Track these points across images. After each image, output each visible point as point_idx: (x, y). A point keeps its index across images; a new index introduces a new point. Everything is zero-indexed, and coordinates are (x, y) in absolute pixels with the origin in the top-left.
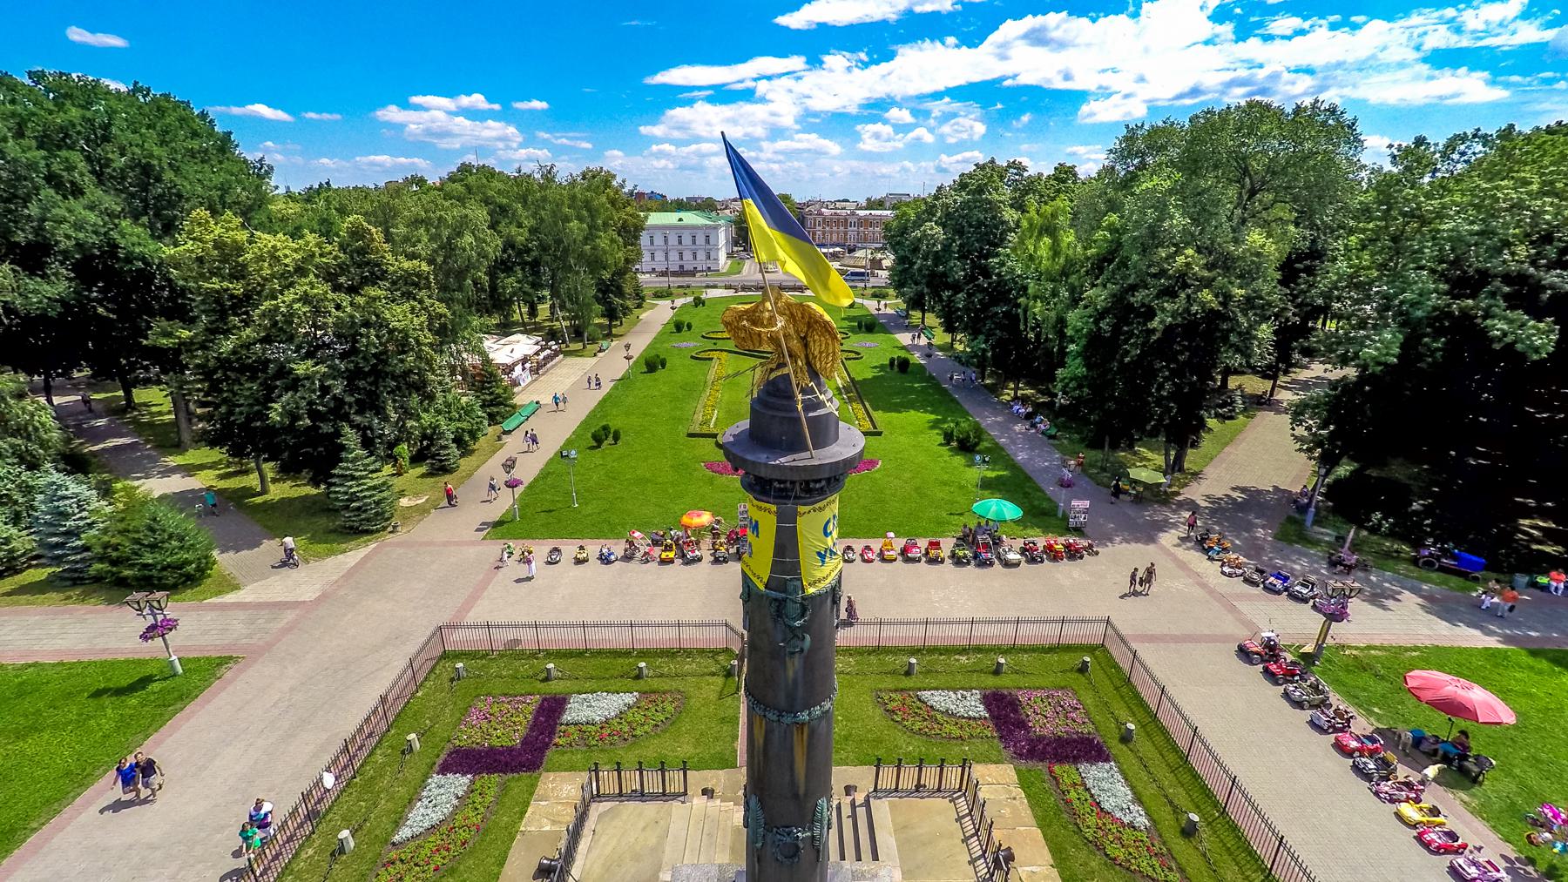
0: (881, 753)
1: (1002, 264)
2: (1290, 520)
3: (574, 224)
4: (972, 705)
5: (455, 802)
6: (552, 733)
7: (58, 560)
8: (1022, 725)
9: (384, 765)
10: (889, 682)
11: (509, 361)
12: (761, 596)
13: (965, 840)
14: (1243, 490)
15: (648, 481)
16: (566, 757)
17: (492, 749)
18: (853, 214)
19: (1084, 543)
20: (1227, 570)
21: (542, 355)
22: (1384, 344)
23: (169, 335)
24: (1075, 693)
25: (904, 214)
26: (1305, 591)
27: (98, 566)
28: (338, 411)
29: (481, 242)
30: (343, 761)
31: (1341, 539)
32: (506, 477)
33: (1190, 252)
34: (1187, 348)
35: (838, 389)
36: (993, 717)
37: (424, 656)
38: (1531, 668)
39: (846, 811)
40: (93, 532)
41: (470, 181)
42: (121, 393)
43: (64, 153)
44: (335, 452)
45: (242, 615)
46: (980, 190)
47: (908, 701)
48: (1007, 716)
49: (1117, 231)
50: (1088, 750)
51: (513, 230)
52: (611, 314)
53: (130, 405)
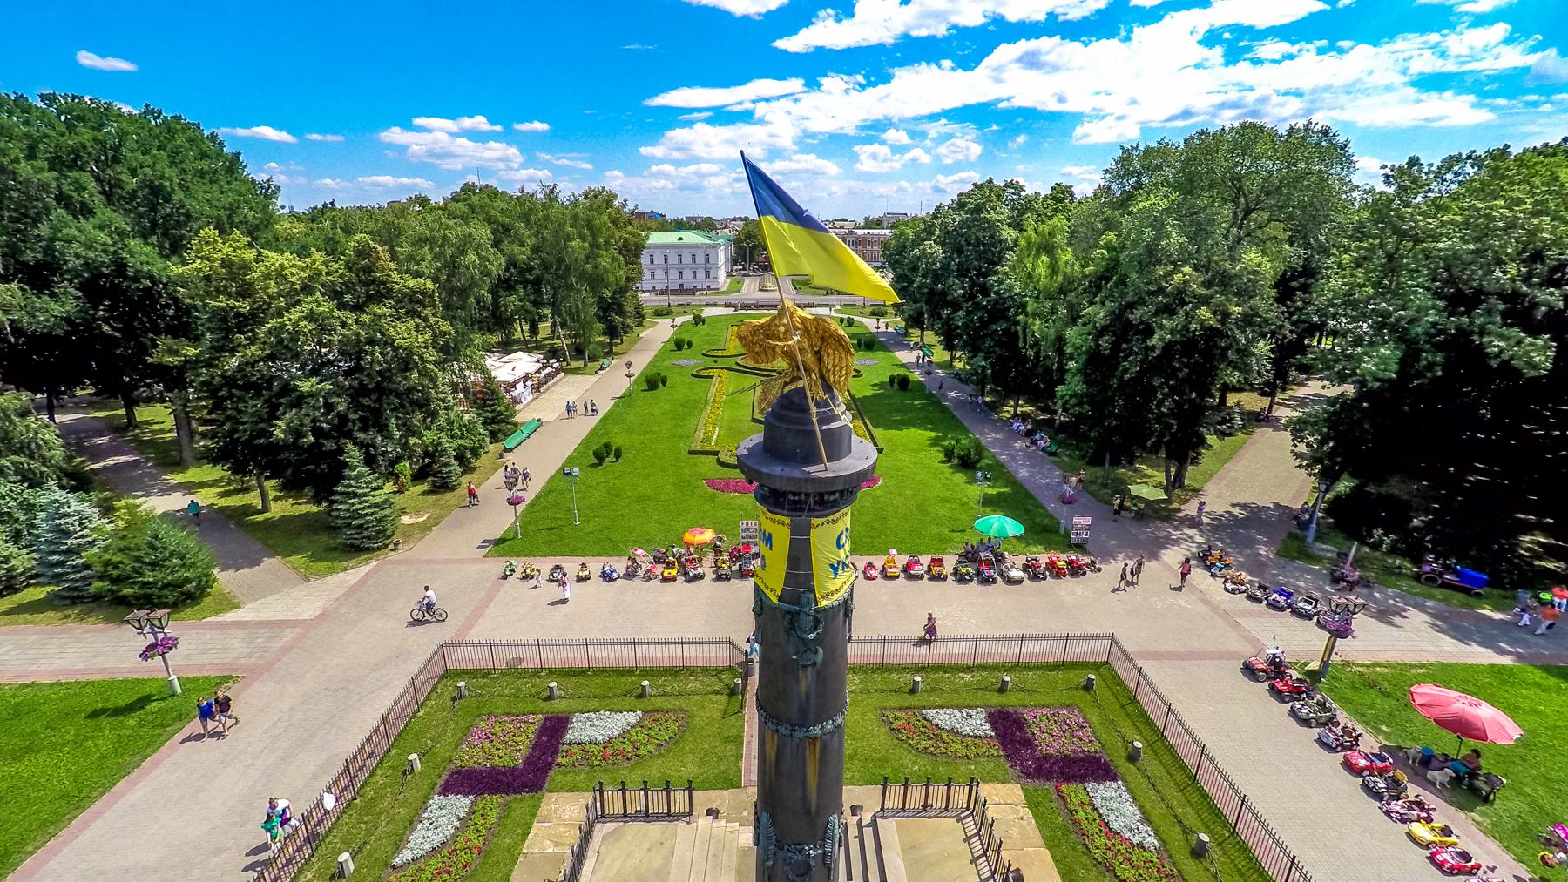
0: (887, 772)
1: (1001, 282)
2: (1292, 536)
3: (575, 243)
4: (977, 723)
5: (457, 823)
6: (555, 752)
7: (58, 578)
8: (1028, 743)
9: (385, 785)
10: (894, 701)
11: (511, 379)
12: (774, 609)
13: (974, 861)
14: (1244, 506)
15: (649, 498)
16: (569, 777)
17: (493, 768)
18: (851, 233)
19: (1087, 560)
20: (1229, 586)
21: (544, 373)
22: (1380, 361)
23: (176, 353)
24: (1081, 711)
25: (903, 233)
26: (1309, 607)
27: (97, 585)
28: (342, 428)
29: (485, 260)
30: (343, 782)
31: (1343, 556)
32: (507, 494)
33: (1187, 269)
34: (1186, 365)
37: (422, 678)
38: (1538, 685)
39: (853, 831)
40: (95, 550)
41: (473, 201)
42: (123, 411)
43: (75, 174)
44: (338, 469)
45: (240, 633)
46: (978, 209)
47: (913, 719)
48: (1013, 734)
49: (1114, 249)
50: (1098, 769)
51: (516, 249)
52: (612, 332)
53: (132, 423)
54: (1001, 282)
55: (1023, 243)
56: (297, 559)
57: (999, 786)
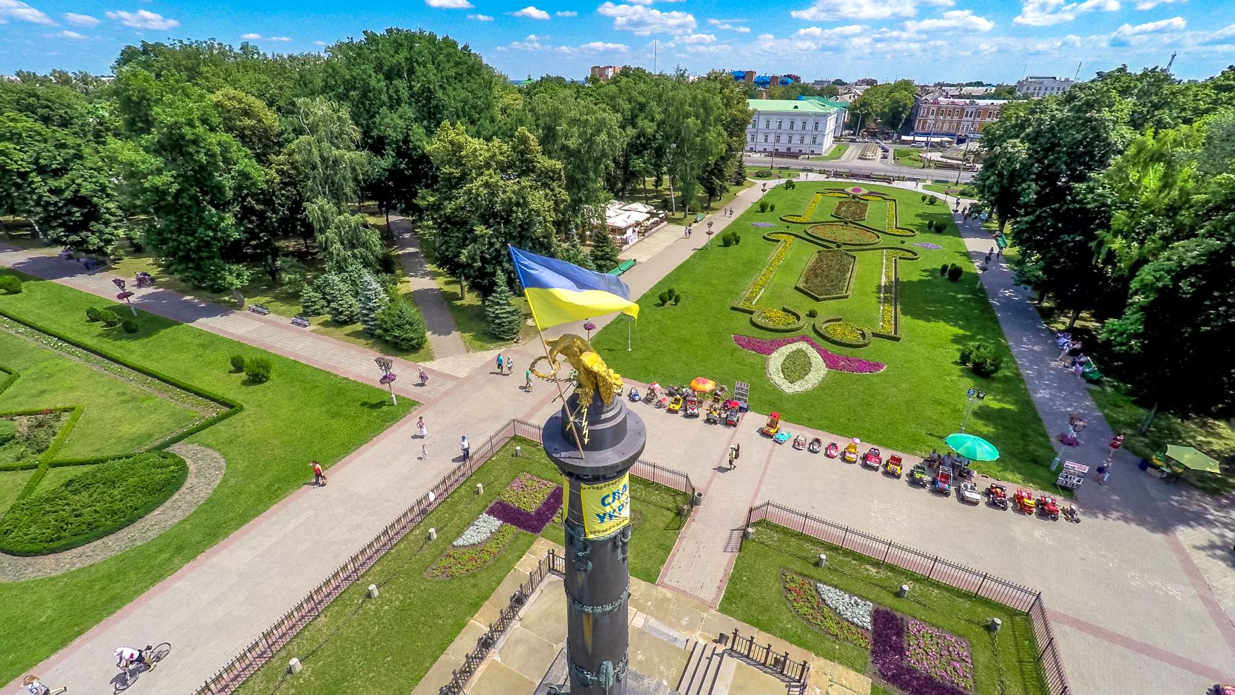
0: (764, 618)
1: (1091, 190)
3: (691, 121)
4: (862, 615)
6: (553, 513)
8: (901, 651)
10: (798, 566)
18: (972, 103)
21: (652, 220)
29: (615, 138)
30: (442, 488)
35: (879, 287)
40: (380, 311)
46: (1089, 105)
51: (647, 123)
52: (712, 192)
54: (1091, 190)
55: (1131, 151)
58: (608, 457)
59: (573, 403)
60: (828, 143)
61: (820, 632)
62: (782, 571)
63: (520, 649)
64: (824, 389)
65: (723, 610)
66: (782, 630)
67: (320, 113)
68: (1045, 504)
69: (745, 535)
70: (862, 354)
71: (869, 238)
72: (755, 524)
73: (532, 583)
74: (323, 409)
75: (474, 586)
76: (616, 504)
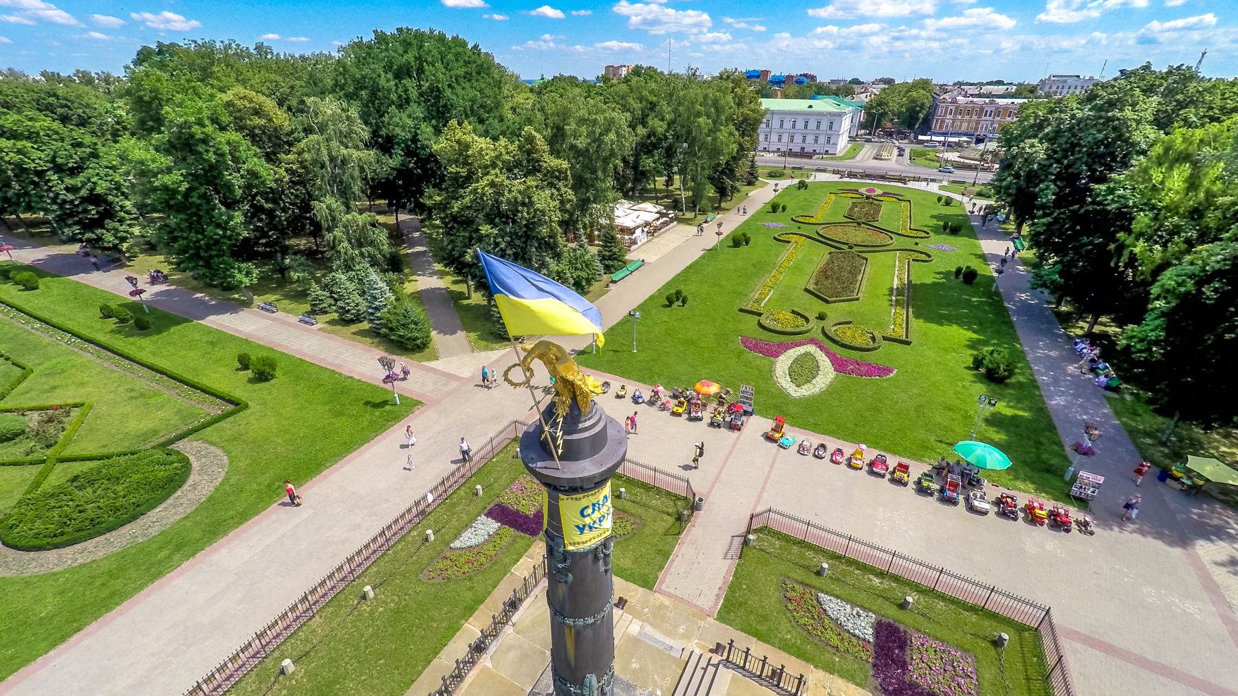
0: (763, 628)
1: (1111, 191)
4: (864, 627)
8: (903, 665)
9: (463, 498)
10: (799, 574)
15: (693, 343)
18: (992, 102)
29: (623, 138)
30: (441, 489)
35: (891, 289)
36: (877, 645)
46: (1111, 104)
47: (807, 596)
52: (722, 192)
54: (1111, 191)
56: (473, 335)
57: (852, 686)
58: (586, 468)
59: (549, 413)
60: (843, 143)
61: (818, 642)
62: (783, 576)
63: (512, 655)
64: (831, 393)
65: (723, 617)
66: (781, 640)
67: (329, 112)
68: (1058, 514)
69: (746, 542)
70: (871, 357)
71: (881, 239)
72: (756, 531)
73: (527, 588)
74: (327, 408)
75: (471, 589)
76: (597, 515)
